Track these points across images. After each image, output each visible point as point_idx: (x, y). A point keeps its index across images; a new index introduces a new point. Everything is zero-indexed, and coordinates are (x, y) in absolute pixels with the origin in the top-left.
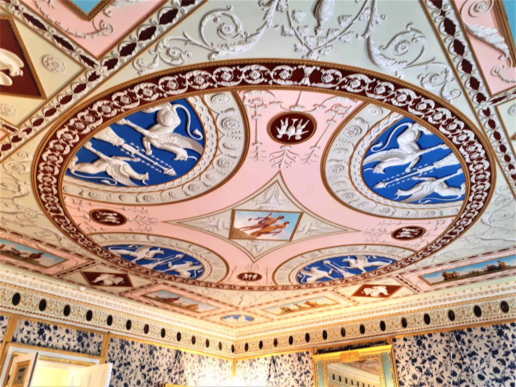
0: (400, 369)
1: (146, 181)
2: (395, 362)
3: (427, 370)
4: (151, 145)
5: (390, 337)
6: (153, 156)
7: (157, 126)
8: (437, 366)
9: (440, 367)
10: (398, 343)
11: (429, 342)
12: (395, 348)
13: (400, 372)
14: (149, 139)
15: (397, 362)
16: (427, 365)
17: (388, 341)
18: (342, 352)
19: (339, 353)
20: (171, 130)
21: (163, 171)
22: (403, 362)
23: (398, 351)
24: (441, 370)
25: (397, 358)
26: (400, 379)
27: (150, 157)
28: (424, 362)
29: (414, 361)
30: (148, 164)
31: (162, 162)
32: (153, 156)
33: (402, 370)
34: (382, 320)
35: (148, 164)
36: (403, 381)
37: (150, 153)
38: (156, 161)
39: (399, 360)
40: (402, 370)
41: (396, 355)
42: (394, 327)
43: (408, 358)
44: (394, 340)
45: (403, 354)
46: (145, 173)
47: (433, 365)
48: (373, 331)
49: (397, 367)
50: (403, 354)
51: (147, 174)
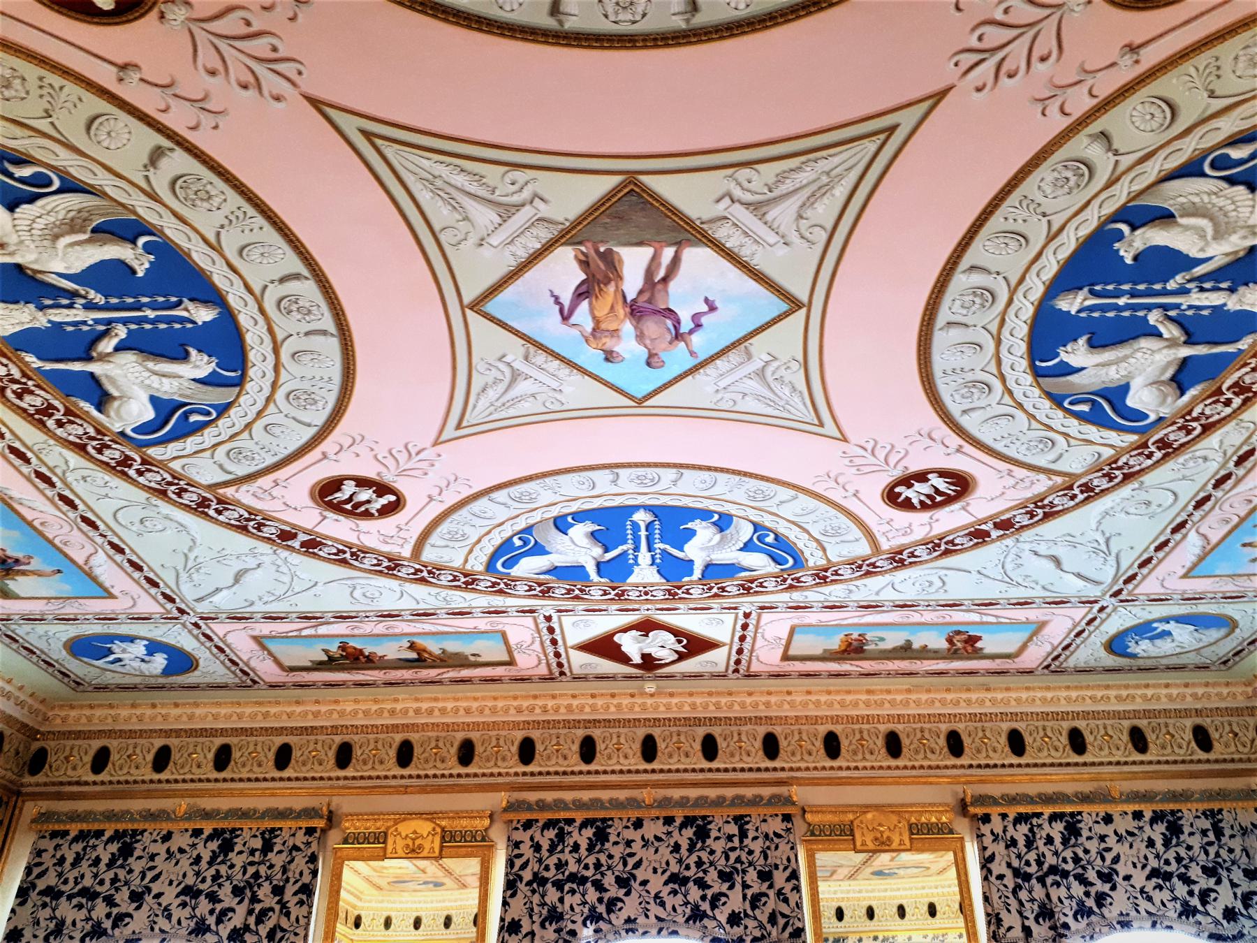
1: (1120, 236)
4: (1160, 335)
6: (1141, 314)
7: (1169, 373)
14: (1173, 343)
20: (1136, 385)
21: (1092, 293)
27: (1149, 308)
30: (1141, 287)
31: (1111, 314)
32: (1141, 314)
35: (1141, 287)
37: (1153, 318)
38: (1128, 307)
46: (1135, 258)
51: (1129, 261)
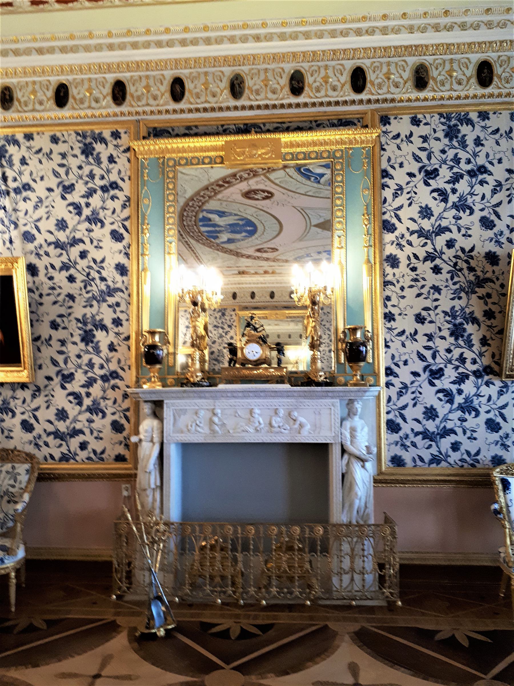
0: (388, 193)
2: (378, 175)
3: (461, 198)
5: (377, 110)
8: (487, 189)
9: (494, 192)
10: (394, 127)
11: (478, 131)
12: (383, 140)
13: (390, 199)
15: (385, 174)
16: (463, 186)
17: (368, 120)
18: (232, 138)
19: (220, 141)
22: (400, 177)
23: (391, 148)
24: (495, 200)
25: (384, 165)
26: (386, 217)
28: (456, 178)
29: (432, 174)
33: (396, 195)
34: (358, 63)
36: (394, 221)
39: (391, 171)
40: (396, 195)
41: (384, 159)
42: (391, 85)
43: (414, 167)
44: (385, 120)
45: (403, 158)
47: (478, 189)
48: (330, 90)
49: (384, 186)
50: (403, 158)
